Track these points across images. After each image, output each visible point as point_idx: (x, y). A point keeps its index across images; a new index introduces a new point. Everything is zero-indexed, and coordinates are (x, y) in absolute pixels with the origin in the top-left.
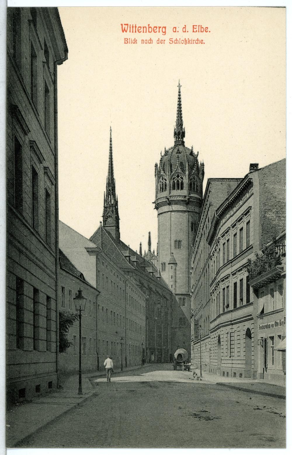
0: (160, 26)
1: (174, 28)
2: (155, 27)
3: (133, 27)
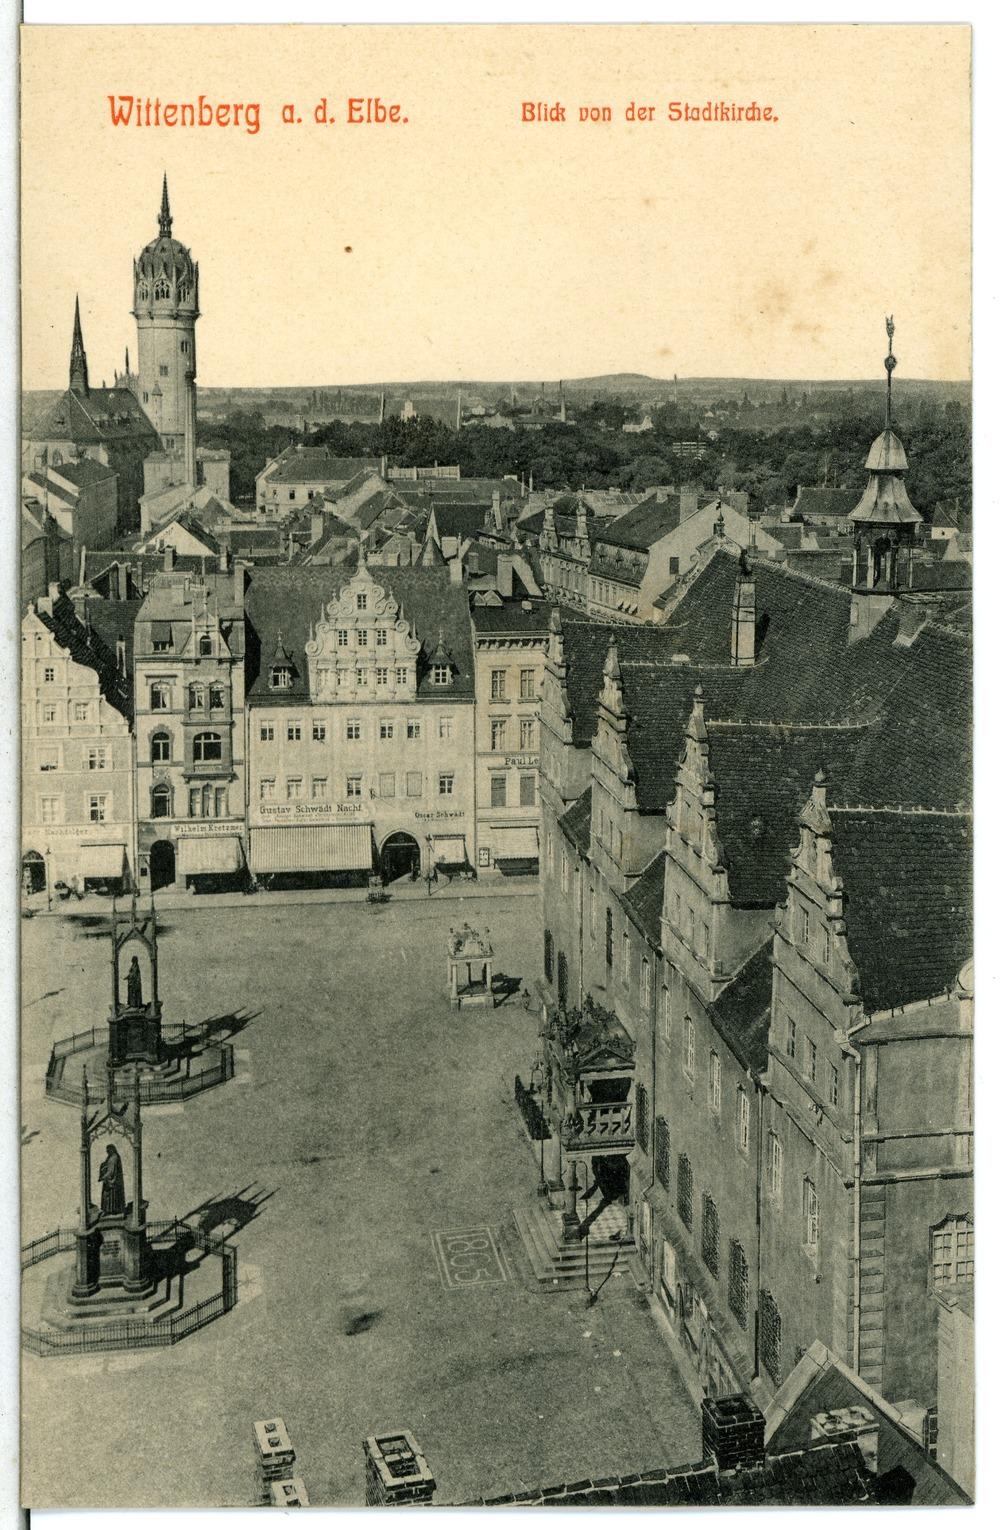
0: (238, 103)
1: (286, 107)
2: (222, 107)
3: (148, 107)
